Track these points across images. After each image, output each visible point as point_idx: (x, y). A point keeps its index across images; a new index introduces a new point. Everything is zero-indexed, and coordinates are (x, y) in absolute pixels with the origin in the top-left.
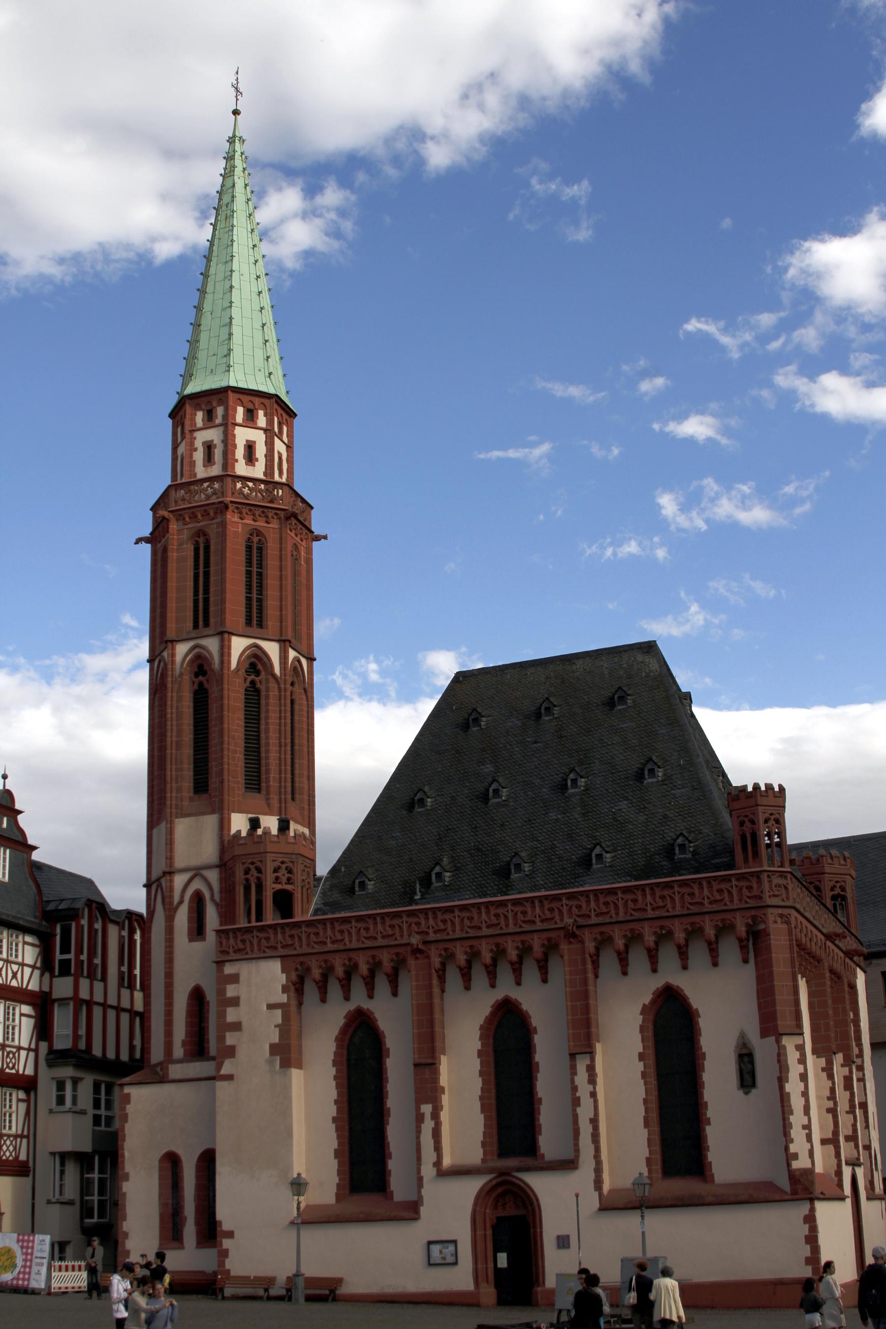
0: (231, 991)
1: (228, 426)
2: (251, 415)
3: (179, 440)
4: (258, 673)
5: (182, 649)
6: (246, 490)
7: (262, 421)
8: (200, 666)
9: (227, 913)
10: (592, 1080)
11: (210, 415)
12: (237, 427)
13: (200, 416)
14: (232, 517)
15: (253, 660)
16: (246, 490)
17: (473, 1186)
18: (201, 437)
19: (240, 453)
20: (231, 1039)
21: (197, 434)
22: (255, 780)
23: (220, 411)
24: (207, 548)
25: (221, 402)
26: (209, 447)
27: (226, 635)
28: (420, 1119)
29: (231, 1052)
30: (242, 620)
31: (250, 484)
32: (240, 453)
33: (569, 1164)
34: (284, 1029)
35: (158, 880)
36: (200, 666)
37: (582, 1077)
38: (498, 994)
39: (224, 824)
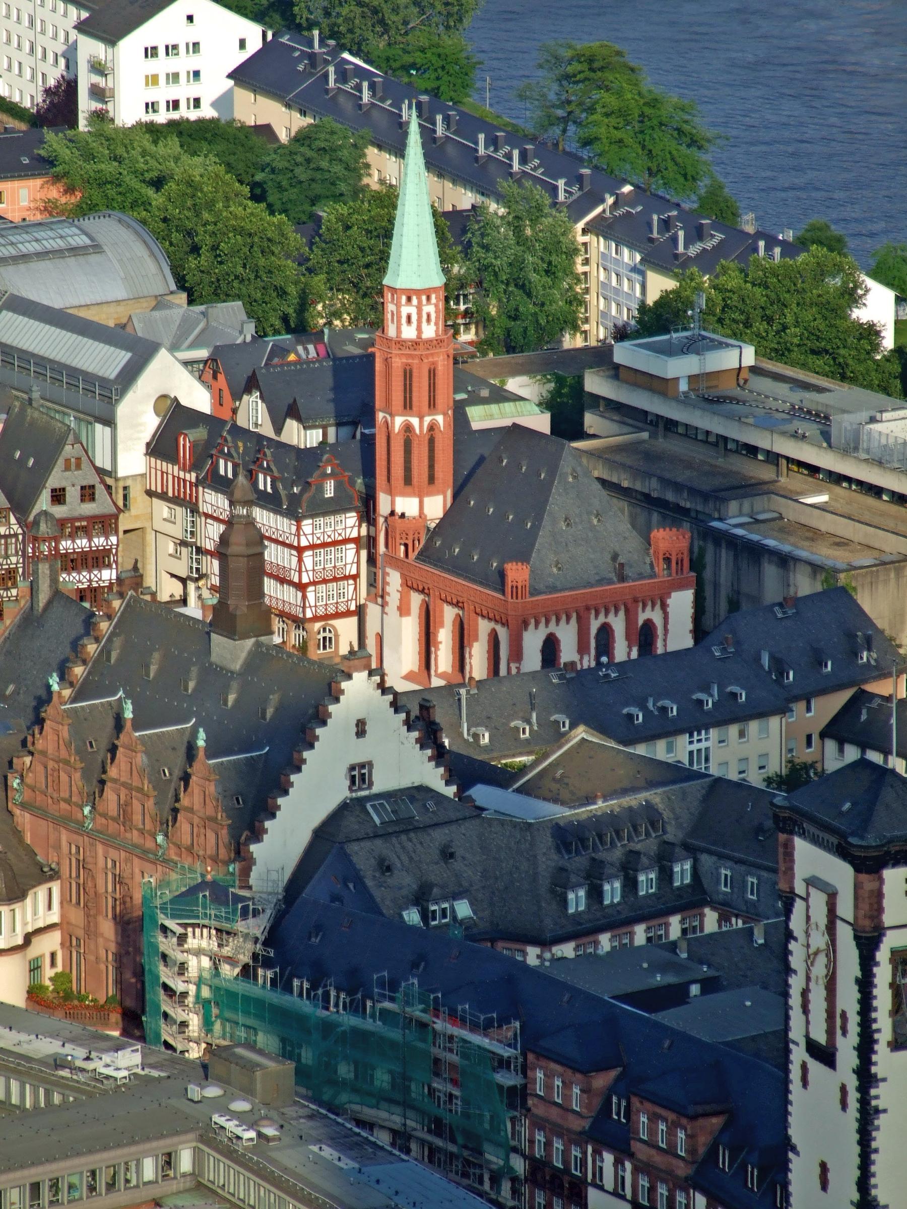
2: (409, 299)
30: (401, 408)
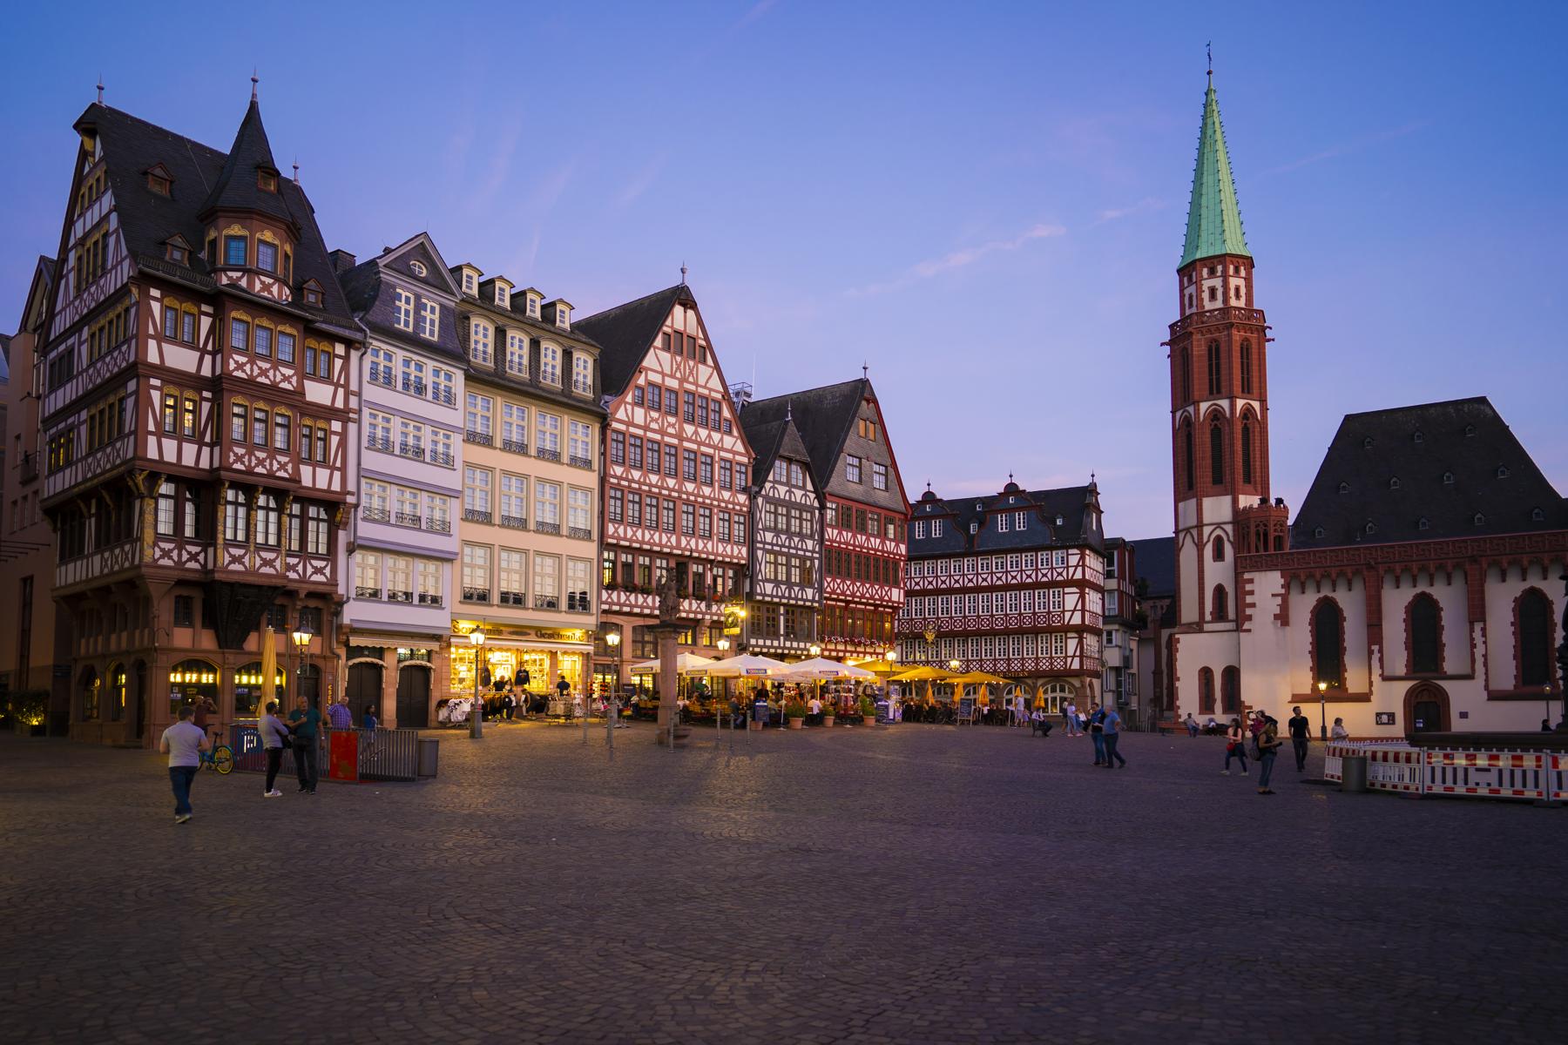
0: (1248, 587)
1: (1225, 277)
2: (1237, 270)
5: (1204, 406)
7: (1243, 273)
8: (1216, 414)
9: (1237, 548)
10: (1484, 635)
11: (1212, 273)
13: (1205, 271)
14: (1234, 332)
17: (1403, 687)
18: (1206, 284)
19: (1232, 293)
20: (1248, 611)
22: (1248, 479)
23: (1220, 268)
24: (1218, 350)
25: (1220, 263)
26: (1213, 291)
28: (1371, 653)
29: (1249, 618)
32: (1232, 293)
33: (1470, 677)
34: (1284, 607)
35: (1188, 530)
36: (1216, 414)
37: (1477, 634)
38: (1419, 590)
39: (1235, 502)
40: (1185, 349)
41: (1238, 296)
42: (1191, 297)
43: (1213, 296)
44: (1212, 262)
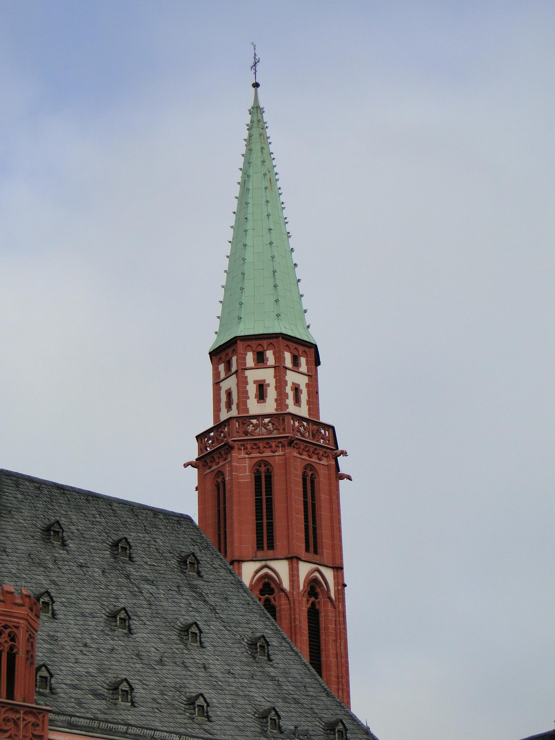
3: (223, 375)
4: (316, 596)
6: (302, 429)
7: (304, 368)
11: (260, 359)
12: (288, 371)
15: (313, 583)
16: (302, 429)
21: (247, 373)
23: (270, 354)
24: (269, 478)
26: (261, 388)
27: (295, 560)
31: (305, 424)
40: (220, 473)
41: (297, 401)
42: (229, 394)
43: (261, 396)
44: (260, 343)
